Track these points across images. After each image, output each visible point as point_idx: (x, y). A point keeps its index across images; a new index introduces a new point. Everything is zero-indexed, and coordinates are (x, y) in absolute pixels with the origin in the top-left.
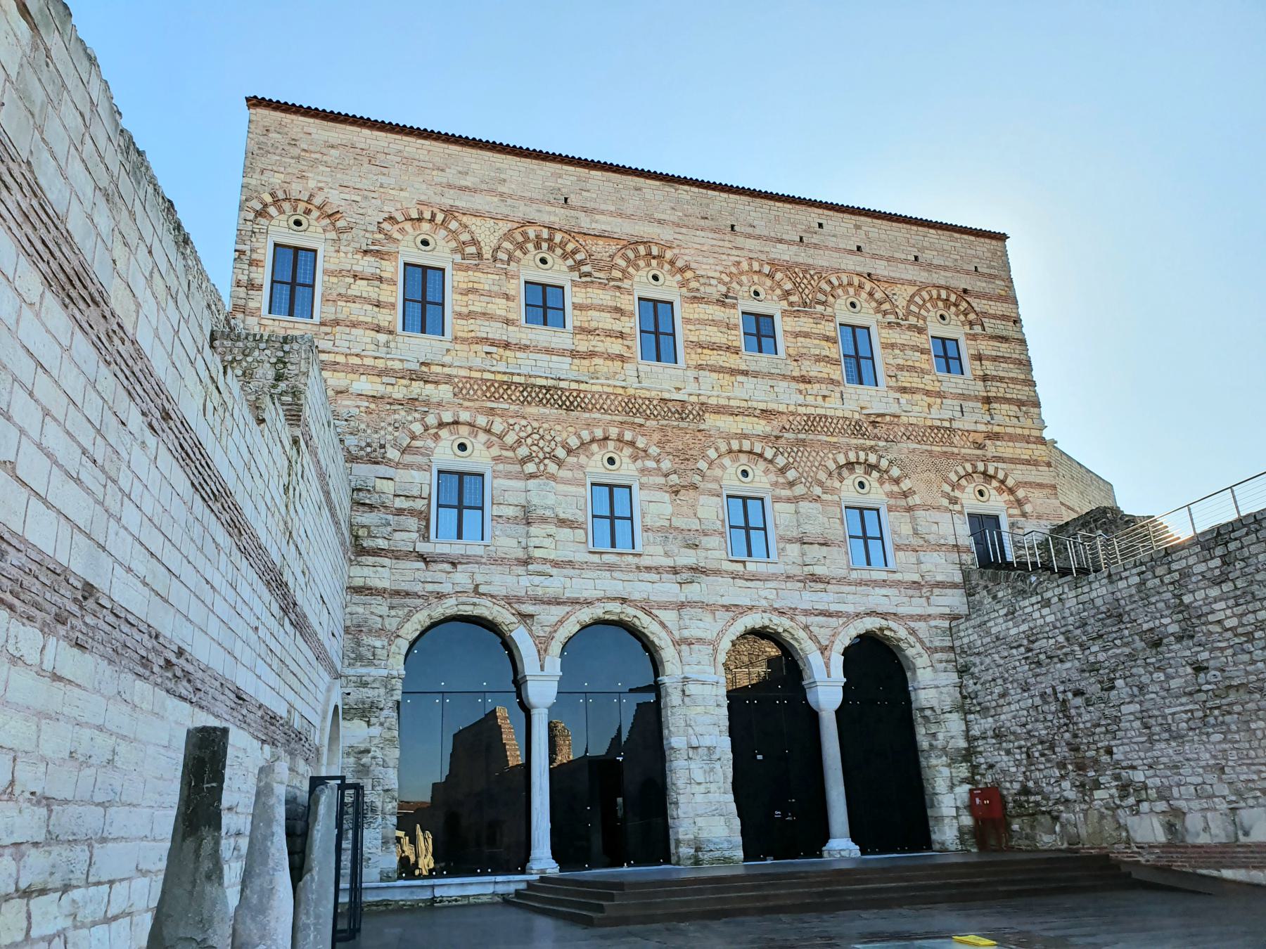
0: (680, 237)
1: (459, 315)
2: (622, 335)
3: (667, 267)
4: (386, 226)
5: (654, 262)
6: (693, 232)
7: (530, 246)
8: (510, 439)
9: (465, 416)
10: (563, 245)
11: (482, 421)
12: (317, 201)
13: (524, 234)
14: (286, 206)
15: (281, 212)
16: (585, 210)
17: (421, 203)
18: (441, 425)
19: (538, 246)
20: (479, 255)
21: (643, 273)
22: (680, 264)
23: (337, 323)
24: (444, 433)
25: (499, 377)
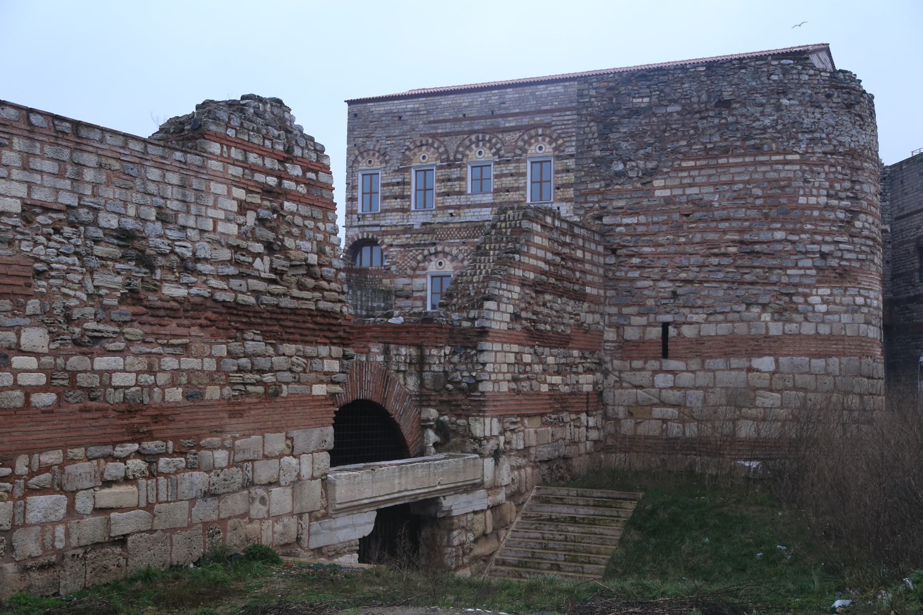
0: (554, 119)
1: (439, 195)
2: (518, 189)
3: (547, 139)
4: (407, 153)
5: (540, 138)
6: (563, 114)
7: (473, 146)
8: (461, 257)
9: (439, 248)
10: (490, 141)
11: (447, 249)
12: (377, 149)
13: (470, 140)
14: (365, 154)
15: (363, 158)
16: (502, 116)
17: (421, 135)
18: (431, 254)
19: (477, 146)
20: (448, 158)
21: (533, 147)
22: (554, 137)
23: (386, 211)
24: (433, 258)
25: (456, 225)
